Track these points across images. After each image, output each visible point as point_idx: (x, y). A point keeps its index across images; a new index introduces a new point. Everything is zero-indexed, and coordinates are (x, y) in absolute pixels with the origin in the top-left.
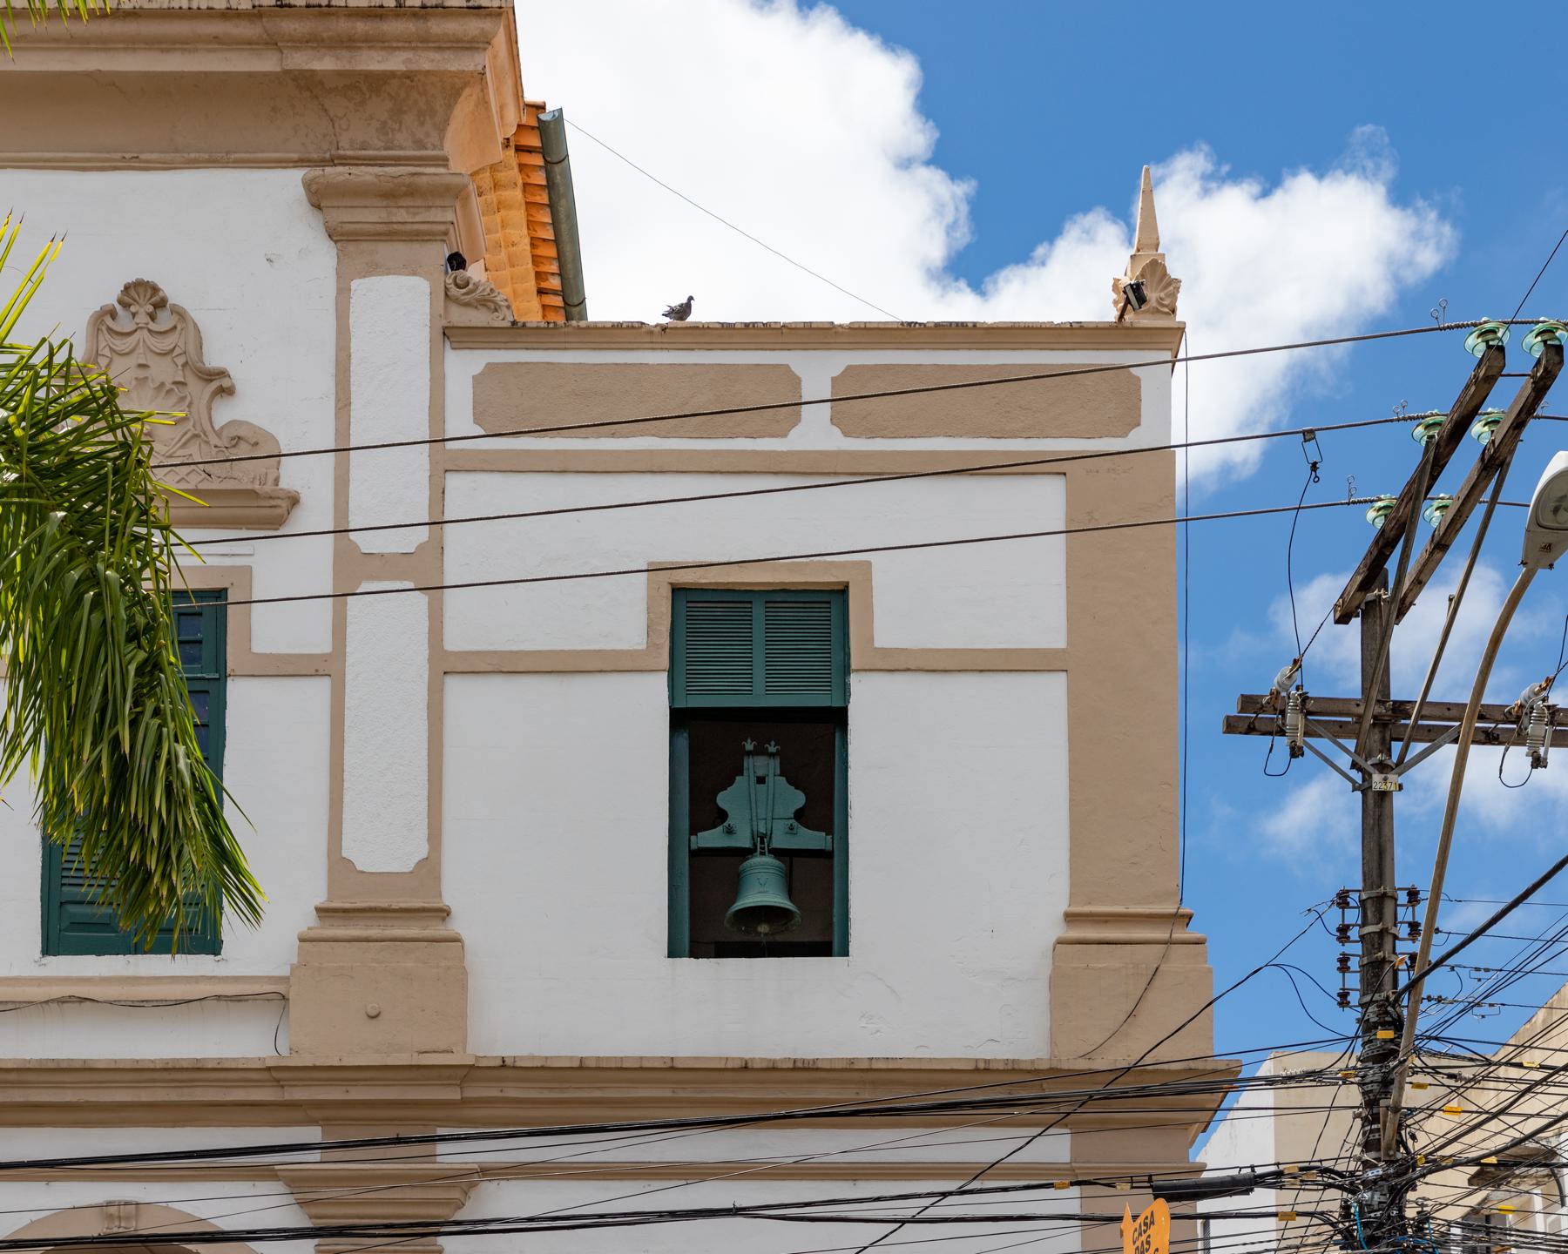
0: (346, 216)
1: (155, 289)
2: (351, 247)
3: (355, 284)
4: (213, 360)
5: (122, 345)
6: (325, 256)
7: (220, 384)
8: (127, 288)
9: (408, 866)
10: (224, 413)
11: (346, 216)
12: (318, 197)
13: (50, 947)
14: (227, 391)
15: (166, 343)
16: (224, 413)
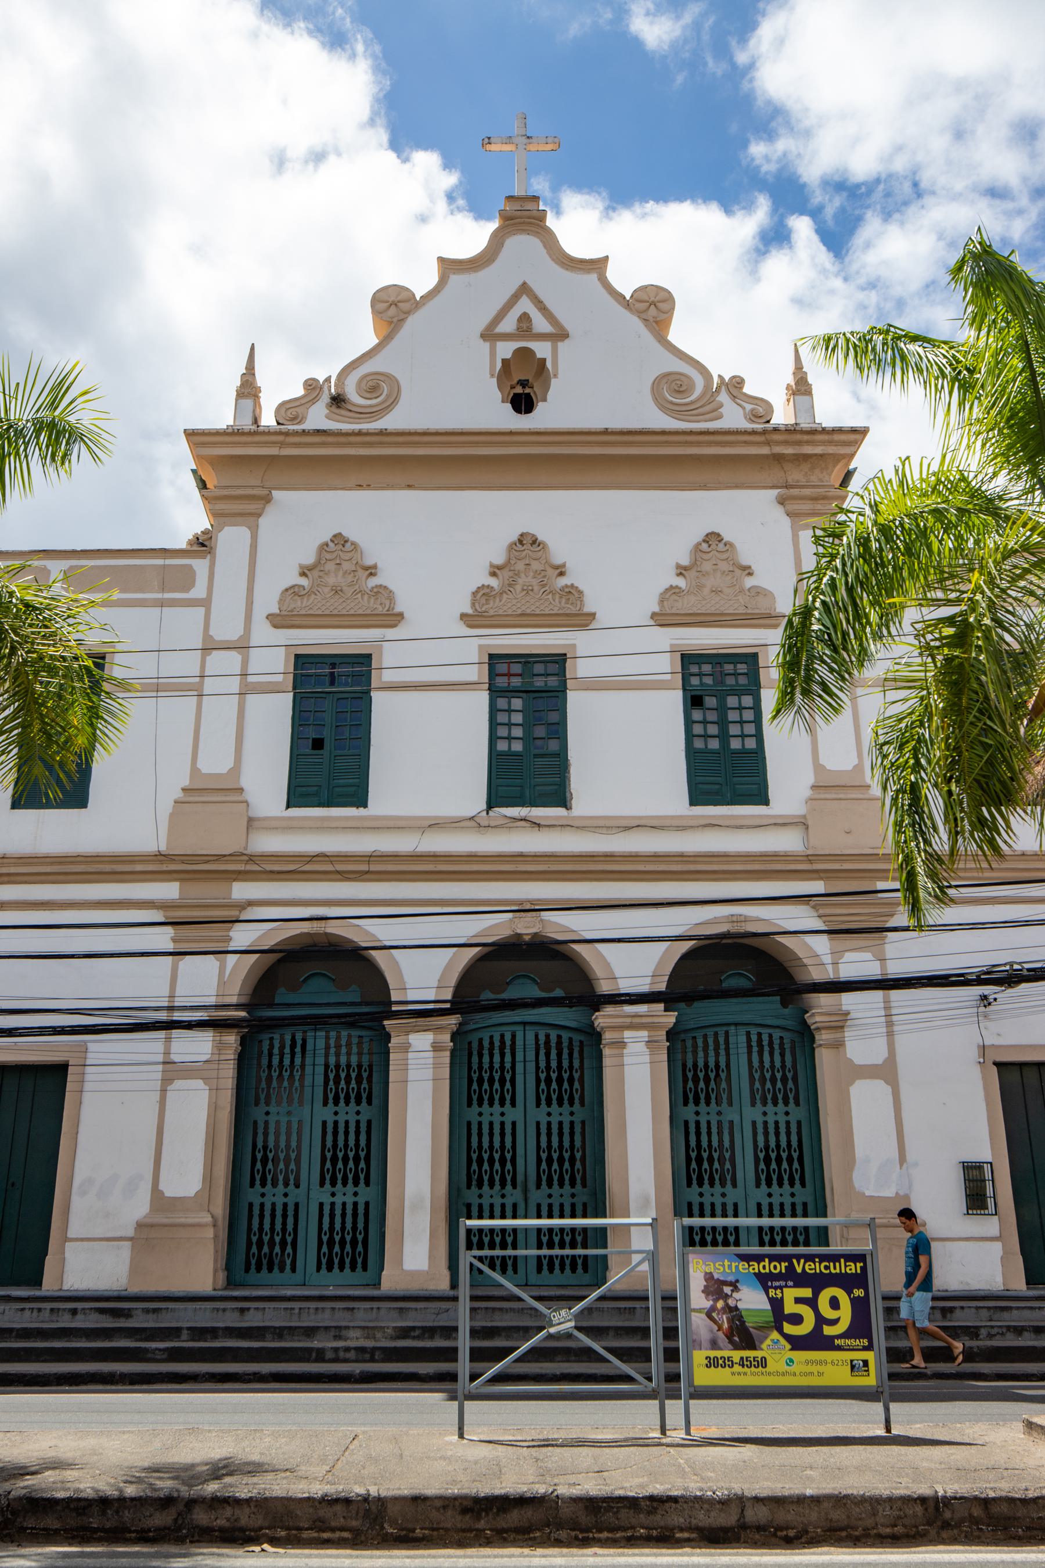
0: (796, 507)
1: (719, 535)
2: (797, 519)
3: (800, 533)
4: (745, 562)
5: (705, 556)
6: (786, 521)
7: (748, 571)
8: (707, 535)
9: (849, 767)
10: (749, 582)
11: (796, 507)
12: (782, 501)
13: (694, 802)
14: (750, 574)
15: (725, 556)
16: (749, 582)
